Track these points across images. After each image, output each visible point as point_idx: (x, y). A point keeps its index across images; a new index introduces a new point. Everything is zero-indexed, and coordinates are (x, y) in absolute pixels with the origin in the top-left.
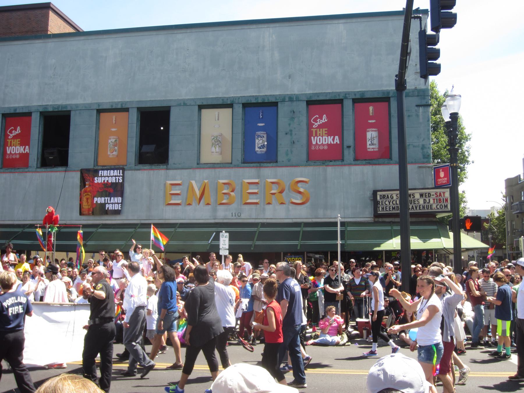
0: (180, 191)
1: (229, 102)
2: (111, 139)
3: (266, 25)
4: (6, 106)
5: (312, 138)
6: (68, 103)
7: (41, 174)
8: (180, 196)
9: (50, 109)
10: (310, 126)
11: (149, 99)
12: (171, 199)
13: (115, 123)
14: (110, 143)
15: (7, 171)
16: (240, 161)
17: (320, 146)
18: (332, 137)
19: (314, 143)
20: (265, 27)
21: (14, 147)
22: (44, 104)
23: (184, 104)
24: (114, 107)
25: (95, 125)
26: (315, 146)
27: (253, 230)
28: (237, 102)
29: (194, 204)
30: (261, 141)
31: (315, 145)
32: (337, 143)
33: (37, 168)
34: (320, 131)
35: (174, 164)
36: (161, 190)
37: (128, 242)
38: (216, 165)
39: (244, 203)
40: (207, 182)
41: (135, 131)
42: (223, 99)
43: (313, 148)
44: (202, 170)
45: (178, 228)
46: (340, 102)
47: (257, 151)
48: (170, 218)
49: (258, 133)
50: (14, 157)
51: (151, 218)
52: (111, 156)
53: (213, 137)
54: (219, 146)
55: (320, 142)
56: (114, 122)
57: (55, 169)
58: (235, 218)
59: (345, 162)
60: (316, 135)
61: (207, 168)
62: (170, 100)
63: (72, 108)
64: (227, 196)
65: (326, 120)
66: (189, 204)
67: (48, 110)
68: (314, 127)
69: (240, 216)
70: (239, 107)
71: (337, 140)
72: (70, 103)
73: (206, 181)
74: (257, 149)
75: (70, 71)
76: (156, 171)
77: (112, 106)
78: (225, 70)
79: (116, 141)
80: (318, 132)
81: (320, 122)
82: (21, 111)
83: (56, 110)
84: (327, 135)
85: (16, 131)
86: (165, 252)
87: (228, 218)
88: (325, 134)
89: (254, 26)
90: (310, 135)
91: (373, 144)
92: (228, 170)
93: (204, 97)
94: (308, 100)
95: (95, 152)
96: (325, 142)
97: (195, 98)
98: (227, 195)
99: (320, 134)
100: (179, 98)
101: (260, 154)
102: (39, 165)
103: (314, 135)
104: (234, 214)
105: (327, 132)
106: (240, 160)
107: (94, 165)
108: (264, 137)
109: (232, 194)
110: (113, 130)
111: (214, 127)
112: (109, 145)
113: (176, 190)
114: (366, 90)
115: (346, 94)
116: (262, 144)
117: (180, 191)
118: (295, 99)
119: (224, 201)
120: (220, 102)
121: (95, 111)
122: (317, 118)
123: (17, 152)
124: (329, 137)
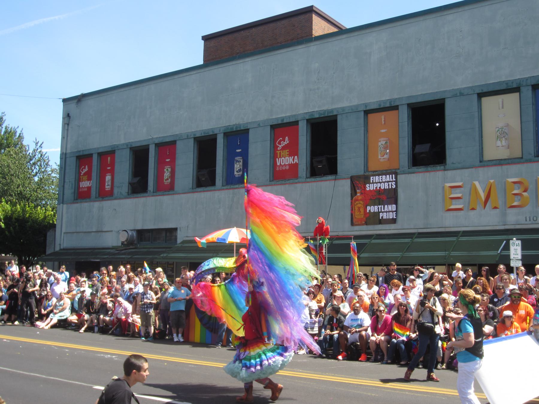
0: (461, 194)
1: (515, 86)
2: (380, 141)
3: (421, 18)
4: (274, 117)
5: (277, 159)
6: (334, 107)
7: (311, 184)
8: (461, 200)
9: (317, 116)
10: (275, 147)
11: (420, 93)
12: (451, 204)
13: (385, 124)
14: (380, 146)
15: (277, 183)
16: (533, 155)
17: (282, 166)
18: (293, 157)
19: (278, 164)
20: (356, 35)
21: (84, 182)
22: (310, 111)
23: (460, 94)
24: (382, 107)
25: (363, 128)
26: (279, 167)
27: (444, 240)
28: (524, 84)
29: (478, 208)
30: (238, 166)
31: (279, 167)
32: (296, 162)
33: (223, 186)
34: (283, 153)
35: (453, 163)
36: (440, 194)
37: (405, 253)
38: (502, 161)
39: (509, 206)
40: (493, 182)
41: (407, 130)
42: (507, 83)
43: (278, 169)
44: (486, 169)
45: (374, 239)
46: (296, 123)
47: (236, 175)
48: (452, 226)
49: (237, 158)
50: (84, 190)
51: (429, 227)
52: (166, 183)
53: (497, 129)
54: (506, 139)
55: (283, 163)
56: (383, 123)
57: (139, 195)
58: (530, 222)
59: (447, 167)
60: (280, 157)
61: (278, 185)
62: (445, 92)
63: (339, 112)
64: (519, 197)
65: (288, 142)
66: (473, 209)
67: (209, 134)
68: (278, 149)
69: (536, 220)
70: (528, 89)
71: (296, 161)
72: (336, 107)
73: (492, 181)
74: (235, 173)
75: (334, 73)
76: (432, 173)
77: (380, 105)
78: (507, 48)
79: (386, 143)
80: (282, 154)
81: (283, 144)
82: (288, 121)
83: (323, 116)
84: (288, 156)
85: (85, 168)
86: (383, 265)
87: (521, 223)
88: (287, 155)
89: (122, 90)
90: (274, 156)
91: (108, 185)
92: (519, 166)
93: (483, 83)
94: (226, 131)
95: (364, 157)
96: (287, 162)
97: (474, 85)
98: (518, 196)
99: (283, 155)
100: (131, 141)
101: (238, 177)
102: (195, 186)
103: (279, 156)
104: (528, 219)
105: (288, 153)
106: (533, 153)
107: (74, 198)
108: (240, 162)
109: (525, 194)
110: (168, 160)
111: (498, 116)
112: (379, 148)
113: (456, 193)
114: (166, 135)
115: (399, 98)
116: (239, 168)
117: (461, 194)
118: (458, 95)
119: (515, 204)
120: (388, 105)
121: (362, 113)
122: (281, 141)
123: (86, 186)
124: (290, 157)
